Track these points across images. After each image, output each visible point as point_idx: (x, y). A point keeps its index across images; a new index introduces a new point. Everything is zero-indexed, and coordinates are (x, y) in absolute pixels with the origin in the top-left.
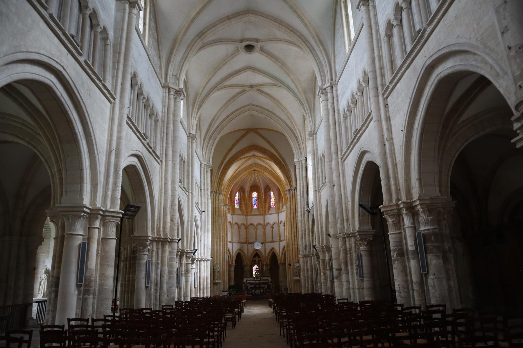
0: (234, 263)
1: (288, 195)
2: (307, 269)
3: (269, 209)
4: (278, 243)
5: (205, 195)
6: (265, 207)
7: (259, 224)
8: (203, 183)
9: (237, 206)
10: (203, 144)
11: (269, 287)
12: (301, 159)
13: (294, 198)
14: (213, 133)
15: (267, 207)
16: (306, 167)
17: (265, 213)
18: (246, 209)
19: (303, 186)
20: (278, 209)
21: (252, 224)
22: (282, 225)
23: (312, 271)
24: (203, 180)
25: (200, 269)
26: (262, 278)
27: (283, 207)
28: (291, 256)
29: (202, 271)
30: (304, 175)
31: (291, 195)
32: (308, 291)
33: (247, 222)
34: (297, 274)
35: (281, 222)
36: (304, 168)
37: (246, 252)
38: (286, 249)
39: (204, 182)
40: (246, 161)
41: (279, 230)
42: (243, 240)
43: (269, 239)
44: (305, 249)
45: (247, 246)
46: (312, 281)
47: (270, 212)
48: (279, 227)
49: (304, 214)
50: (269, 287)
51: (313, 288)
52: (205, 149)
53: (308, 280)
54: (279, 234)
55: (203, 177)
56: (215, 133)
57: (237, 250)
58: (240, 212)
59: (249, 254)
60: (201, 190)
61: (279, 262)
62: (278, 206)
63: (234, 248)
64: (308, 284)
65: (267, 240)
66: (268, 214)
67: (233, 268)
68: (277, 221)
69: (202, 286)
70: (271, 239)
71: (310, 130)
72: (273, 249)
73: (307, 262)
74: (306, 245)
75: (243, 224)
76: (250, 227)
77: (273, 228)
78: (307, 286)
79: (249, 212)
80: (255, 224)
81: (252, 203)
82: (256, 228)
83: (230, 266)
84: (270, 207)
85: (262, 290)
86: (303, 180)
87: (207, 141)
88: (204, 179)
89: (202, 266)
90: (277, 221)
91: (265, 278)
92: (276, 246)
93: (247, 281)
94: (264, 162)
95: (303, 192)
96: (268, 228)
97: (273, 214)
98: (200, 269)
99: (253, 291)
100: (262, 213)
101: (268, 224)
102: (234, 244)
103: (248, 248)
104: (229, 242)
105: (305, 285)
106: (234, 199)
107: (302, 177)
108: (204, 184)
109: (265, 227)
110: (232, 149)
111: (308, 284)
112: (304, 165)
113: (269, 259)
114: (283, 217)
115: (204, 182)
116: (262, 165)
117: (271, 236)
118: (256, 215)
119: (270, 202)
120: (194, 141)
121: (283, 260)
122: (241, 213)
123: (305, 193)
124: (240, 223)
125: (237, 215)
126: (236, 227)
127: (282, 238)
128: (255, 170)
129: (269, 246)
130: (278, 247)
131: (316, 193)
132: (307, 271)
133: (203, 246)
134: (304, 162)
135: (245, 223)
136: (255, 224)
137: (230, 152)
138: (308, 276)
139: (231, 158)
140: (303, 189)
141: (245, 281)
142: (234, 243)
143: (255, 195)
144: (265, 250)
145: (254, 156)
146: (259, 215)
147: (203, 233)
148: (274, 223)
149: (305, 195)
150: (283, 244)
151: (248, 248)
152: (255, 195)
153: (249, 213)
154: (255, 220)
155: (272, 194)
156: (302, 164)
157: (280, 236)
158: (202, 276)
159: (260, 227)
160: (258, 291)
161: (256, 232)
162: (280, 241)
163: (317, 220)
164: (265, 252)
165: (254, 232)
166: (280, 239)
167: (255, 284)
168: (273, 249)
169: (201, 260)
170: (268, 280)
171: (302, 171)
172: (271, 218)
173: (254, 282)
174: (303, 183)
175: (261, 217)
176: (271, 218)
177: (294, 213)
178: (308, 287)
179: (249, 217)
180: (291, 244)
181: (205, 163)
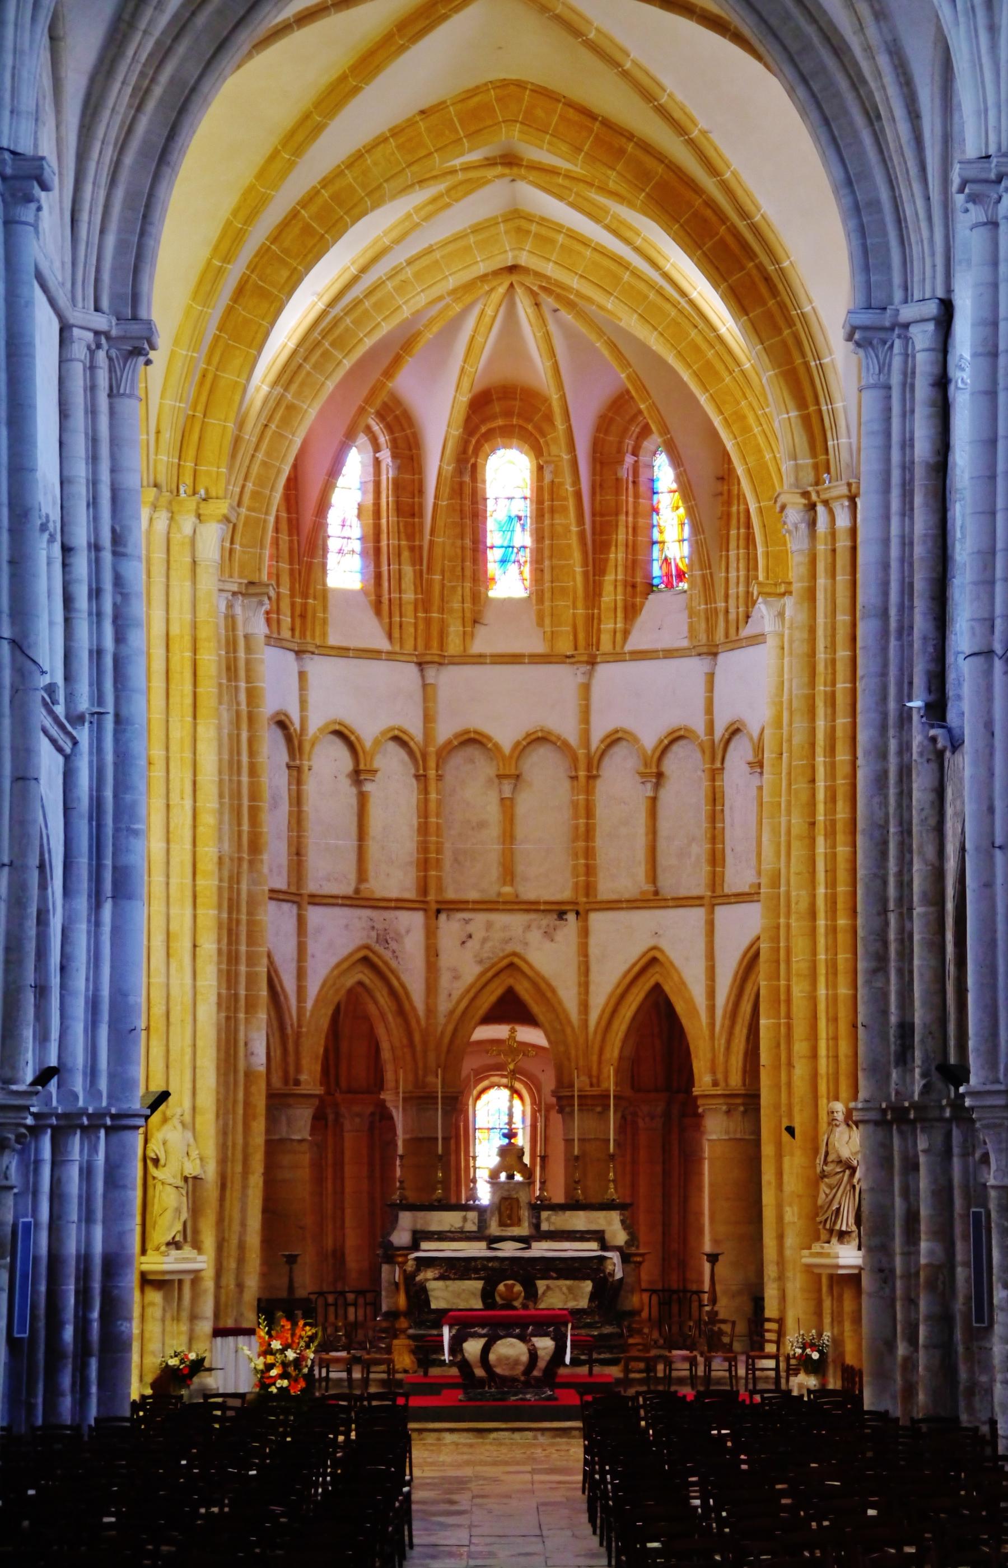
0: (310, 1079)
1: (796, 544)
2: (912, 1218)
3: (631, 612)
4: (696, 915)
5: (96, 593)
6: (593, 592)
7: (539, 739)
8: (81, 490)
9: (345, 570)
10: (82, 157)
11: (607, 1293)
12: (907, 313)
13: (842, 578)
14: (162, 54)
15: (611, 594)
16: (942, 382)
17: (593, 640)
18: (424, 604)
19: (907, 543)
20: (711, 616)
21: (472, 740)
22: (739, 754)
23: (944, 1234)
24: (80, 470)
25: (57, 1195)
26: (550, 1221)
27: (750, 602)
28: (800, 1070)
29: (73, 1213)
30: (923, 449)
31: (822, 547)
32: (909, 1392)
33: (428, 718)
34: (847, 1222)
35: (735, 731)
36: (923, 390)
37: (413, 979)
38: (762, 979)
39: (94, 483)
40: (438, 205)
41: (715, 798)
42: (393, 879)
43: (620, 873)
44: (904, 1057)
45: (431, 934)
46: (943, 1320)
47: (637, 641)
48: (715, 774)
49: (905, 772)
50: (607, 1293)
51: (946, 1368)
52: (93, 194)
53: (911, 1302)
54: (715, 837)
55: (79, 446)
56: (181, 49)
57: (344, 967)
58: (372, 634)
59: (444, 1006)
60: (67, 550)
61: (703, 1081)
62: (707, 586)
64: (912, 1339)
65: (606, 888)
66: (618, 657)
67: (300, 1124)
68: (699, 726)
69: (69, 1333)
70: (641, 871)
71: (971, 147)
72: (652, 961)
73: (911, 1166)
74: (906, 1029)
75: (400, 740)
76: (457, 760)
77: (660, 775)
78: (902, 1349)
79: (455, 629)
80: (505, 736)
81: (476, 549)
82: (511, 775)
83: (278, 1102)
84: (639, 588)
85: (545, 1344)
86: (907, 495)
87: (109, 126)
88: (94, 459)
89: (74, 1172)
90: (699, 726)
91: (579, 1221)
92: (679, 935)
93: (419, 1236)
94: (595, 215)
95: (907, 589)
96: (620, 784)
97: (669, 654)
98: (57, 1195)
99: (473, 1347)
100: (565, 646)
101: (614, 739)
102: (315, 915)
103: (432, 952)
104: (275, 895)
105: (890, 1345)
106: (323, 506)
107: (907, 467)
108: (93, 503)
109: (586, 768)
110: (318, 129)
111: (912, 1339)
112: (924, 363)
113: (613, 1051)
114: (756, 683)
115: (94, 483)
116: (573, 235)
117: (641, 853)
118: (515, 659)
119: (642, 542)
120: (27, 213)
121: (737, 1061)
122: (382, 643)
123: (920, 606)
124: (368, 730)
125: (343, 652)
126: (329, 763)
127: (738, 876)
128: (513, 269)
129: (619, 943)
130: (701, 959)
131: (989, 672)
132: (912, 1235)
133: (79, 1008)
134: (923, 336)
135: (415, 729)
136: (505, 736)
137: (299, 151)
138: (911, 1276)
139: (305, 203)
140: (906, 560)
141: (401, 1237)
142: (317, 900)
143: (508, 476)
144: (585, 970)
145: (509, 160)
146: (537, 659)
147: (82, 903)
148: (676, 738)
149: (921, 623)
150: (740, 926)
151: (432, 952)
152: (508, 476)
153: (454, 646)
154: (501, 702)
155: (664, 473)
156: (907, 356)
157: (716, 859)
158: (71, 1247)
159: (545, 772)
160: (510, 1349)
161: (508, 806)
162: (716, 896)
163: (988, 885)
164: (584, 986)
165: (492, 811)
166: (715, 880)
167: (490, 1272)
168: (652, 961)
169: (65, 1126)
170: (598, 1236)
171: (907, 414)
172: (645, 695)
173: (476, 1249)
174: (907, 510)
175: (565, 678)
176: (645, 695)
177: (842, 701)
178: (909, 1364)
179: (450, 680)
180: (799, 962)
181: (101, 322)
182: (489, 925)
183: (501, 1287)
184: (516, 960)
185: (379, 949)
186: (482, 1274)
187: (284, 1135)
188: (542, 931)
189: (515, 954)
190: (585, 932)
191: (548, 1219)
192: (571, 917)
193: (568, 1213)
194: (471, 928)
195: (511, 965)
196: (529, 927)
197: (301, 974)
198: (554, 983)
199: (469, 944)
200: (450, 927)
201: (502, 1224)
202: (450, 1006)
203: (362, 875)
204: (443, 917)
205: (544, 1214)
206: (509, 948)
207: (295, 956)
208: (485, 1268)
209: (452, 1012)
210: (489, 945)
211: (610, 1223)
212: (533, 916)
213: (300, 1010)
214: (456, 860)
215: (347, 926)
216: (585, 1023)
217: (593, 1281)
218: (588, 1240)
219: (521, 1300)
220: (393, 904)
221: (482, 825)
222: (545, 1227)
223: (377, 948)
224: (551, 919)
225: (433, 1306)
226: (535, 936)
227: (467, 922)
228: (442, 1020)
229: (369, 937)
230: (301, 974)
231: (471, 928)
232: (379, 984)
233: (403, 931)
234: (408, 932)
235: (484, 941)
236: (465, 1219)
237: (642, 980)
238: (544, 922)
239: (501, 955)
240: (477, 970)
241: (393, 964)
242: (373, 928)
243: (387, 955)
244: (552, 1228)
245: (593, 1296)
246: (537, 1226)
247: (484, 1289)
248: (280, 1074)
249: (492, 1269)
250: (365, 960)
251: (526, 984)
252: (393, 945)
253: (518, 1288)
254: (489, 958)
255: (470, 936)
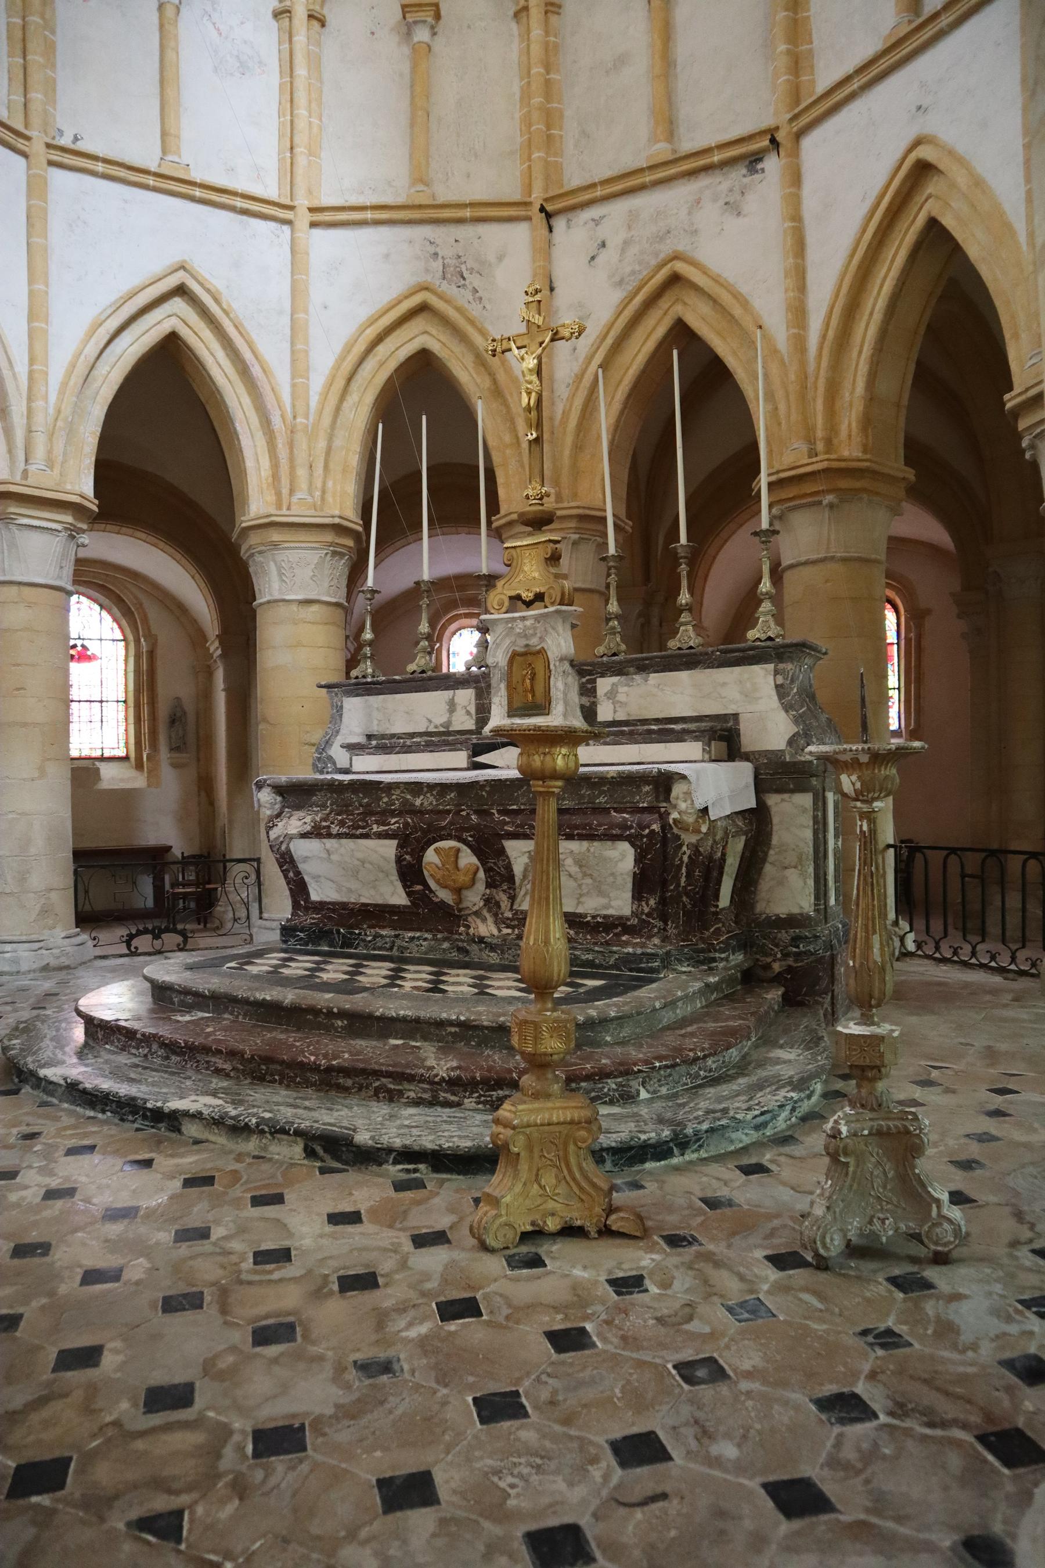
63: (318, 292)
142: (324, 218)
182: (632, 218)
183: (430, 856)
184: (680, 267)
185: (448, 289)
186: (395, 823)
187: (277, 596)
188: (721, 202)
189: (676, 257)
190: (795, 178)
191: (611, 695)
192: (772, 164)
193: (654, 678)
194: (603, 232)
195: (675, 279)
196: (698, 201)
197: (297, 331)
198: (744, 289)
199: (603, 257)
200: (572, 236)
201: (511, 713)
202: (576, 367)
203: (420, 178)
204: (560, 224)
205: (604, 684)
206: (666, 249)
207: (287, 305)
208: (408, 809)
209: (580, 377)
210: (634, 250)
211: (749, 696)
212: (704, 182)
213: (298, 391)
214: (584, 134)
215: (387, 256)
216: (799, 343)
217: (631, 840)
218: (679, 737)
219: (481, 886)
220: (467, 213)
221: (621, 61)
222: (605, 713)
223: (445, 287)
224: (738, 175)
225: (314, 897)
226: (710, 214)
227: (597, 222)
228: (562, 391)
229: (427, 271)
230: (297, 331)
231: (603, 232)
232: (458, 348)
233: (492, 258)
234: (500, 258)
235: (627, 243)
236: (452, 706)
237: (902, 225)
238: (726, 185)
239: (653, 262)
240: (617, 296)
241: (475, 310)
242: (436, 254)
243: (463, 297)
244: (621, 716)
245: (642, 885)
246: (589, 713)
247: (399, 860)
248: (271, 497)
249: (419, 812)
250: (423, 308)
251: (704, 308)
252: (473, 280)
253: (468, 859)
254: (633, 272)
255: (604, 245)
